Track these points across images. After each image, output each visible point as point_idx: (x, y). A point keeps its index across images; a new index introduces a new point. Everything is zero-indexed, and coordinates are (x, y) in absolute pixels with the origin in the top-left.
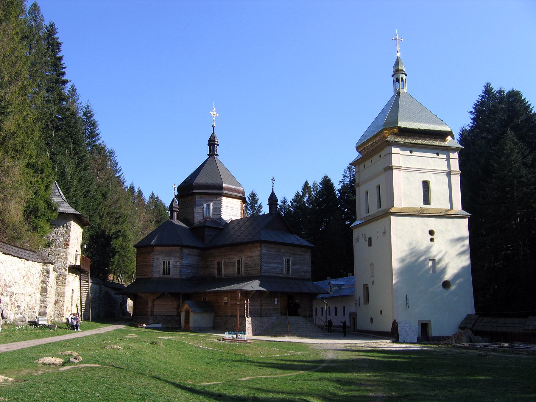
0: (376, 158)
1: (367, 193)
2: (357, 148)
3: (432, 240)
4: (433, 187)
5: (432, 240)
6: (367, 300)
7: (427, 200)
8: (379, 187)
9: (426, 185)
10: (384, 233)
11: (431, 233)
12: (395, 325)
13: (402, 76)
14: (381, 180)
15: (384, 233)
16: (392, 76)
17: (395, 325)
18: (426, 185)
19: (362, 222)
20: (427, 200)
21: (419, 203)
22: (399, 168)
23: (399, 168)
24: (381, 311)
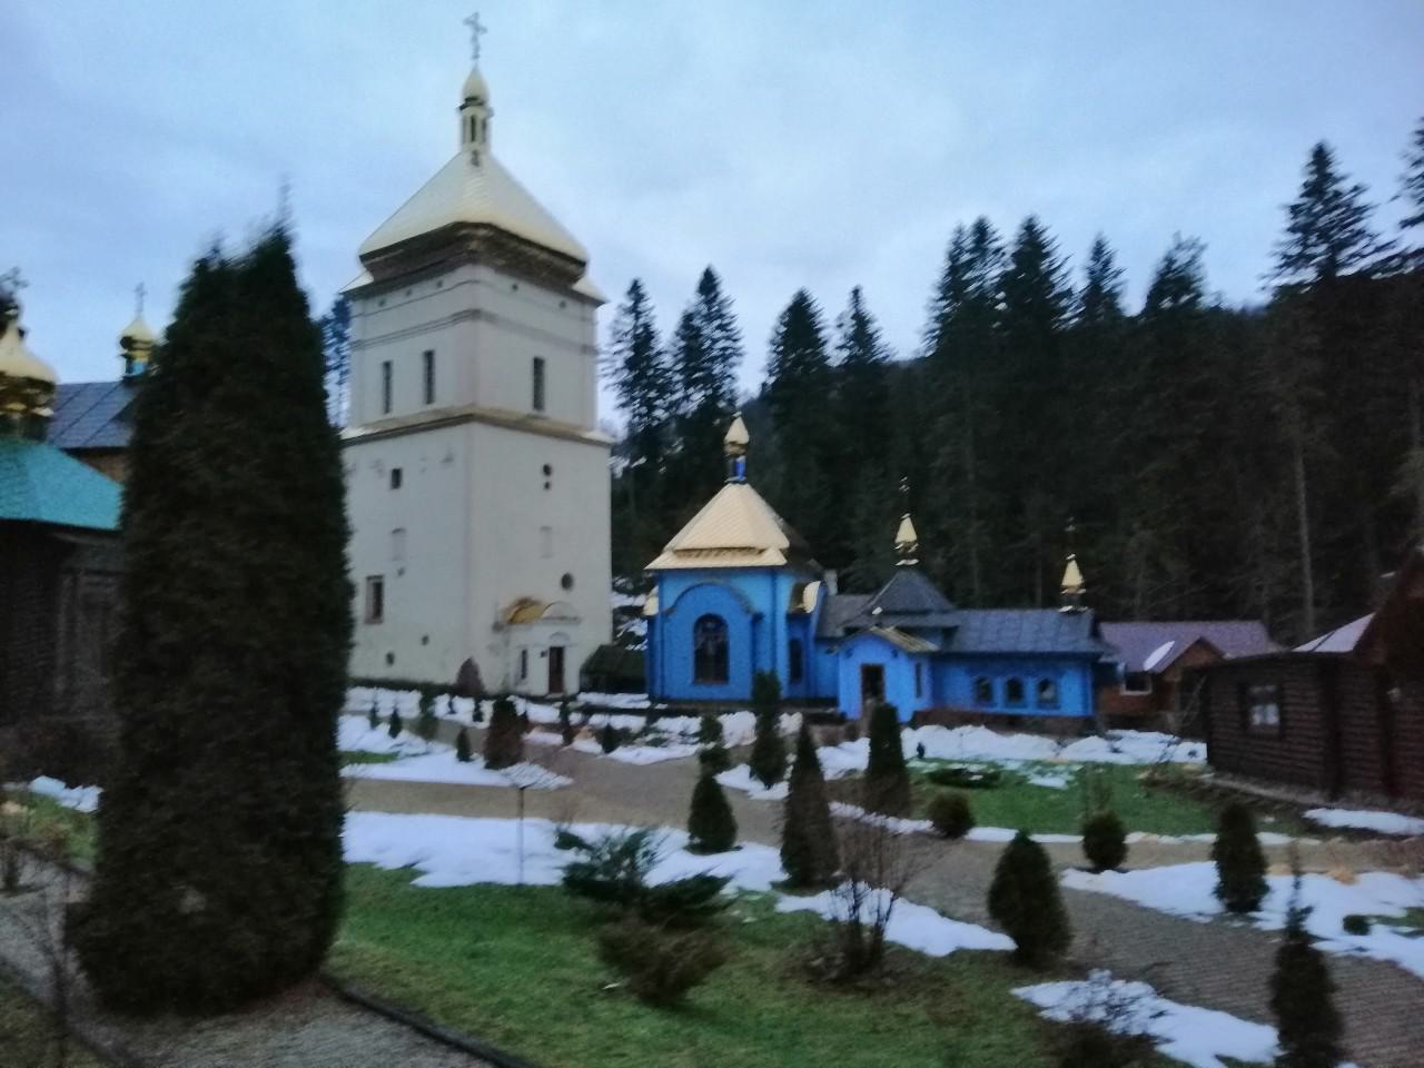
0: (427, 288)
1: (387, 365)
2: (364, 258)
3: (547, 486)
4: (550, 373)
5: (547, 486)
6: (377, 612)
7: (538, 402)
8: (429, 356)
9: (538, 364)
10: (448, 460)
11: (547, 470)
12: (469, 669)
13: (480, 114)
14: (437, 341)
15: (448, 460)
16: (462, 108)
17: (469, 669)
18: (538, 364)
19: (369, 432)
20: (538, 402)
21: (522, 404)
22: (491, 318)
23: (491, 318)
24: (425, 640)
